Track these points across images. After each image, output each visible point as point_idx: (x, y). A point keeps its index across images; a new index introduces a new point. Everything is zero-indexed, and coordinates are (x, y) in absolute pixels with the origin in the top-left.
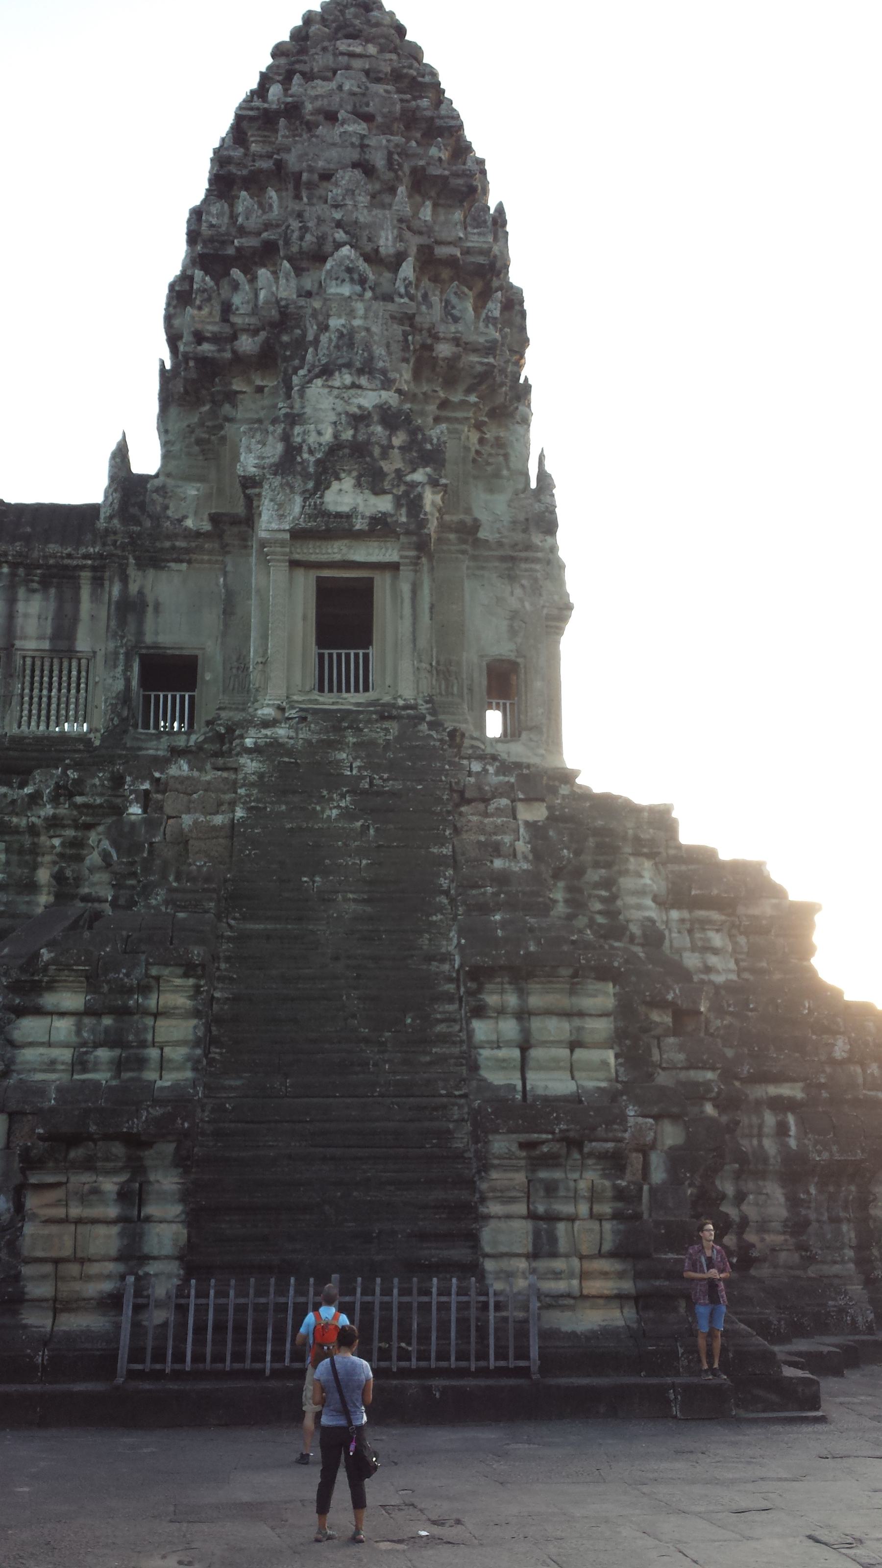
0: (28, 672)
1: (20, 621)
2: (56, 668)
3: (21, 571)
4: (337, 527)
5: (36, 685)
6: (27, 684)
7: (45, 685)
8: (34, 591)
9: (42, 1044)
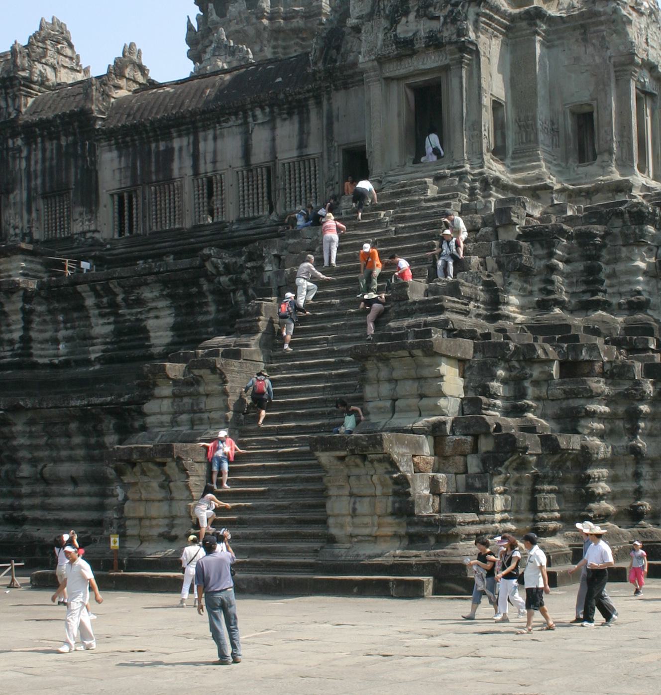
0: (287, 173)
1: (278, 141)
2: (302, 167)
3: (276, 110)
4: (406, 48)
5: (292, 180)
6: (287, 181)
7: (297, 179)
8: (285, 119)
9: (158, 413)
